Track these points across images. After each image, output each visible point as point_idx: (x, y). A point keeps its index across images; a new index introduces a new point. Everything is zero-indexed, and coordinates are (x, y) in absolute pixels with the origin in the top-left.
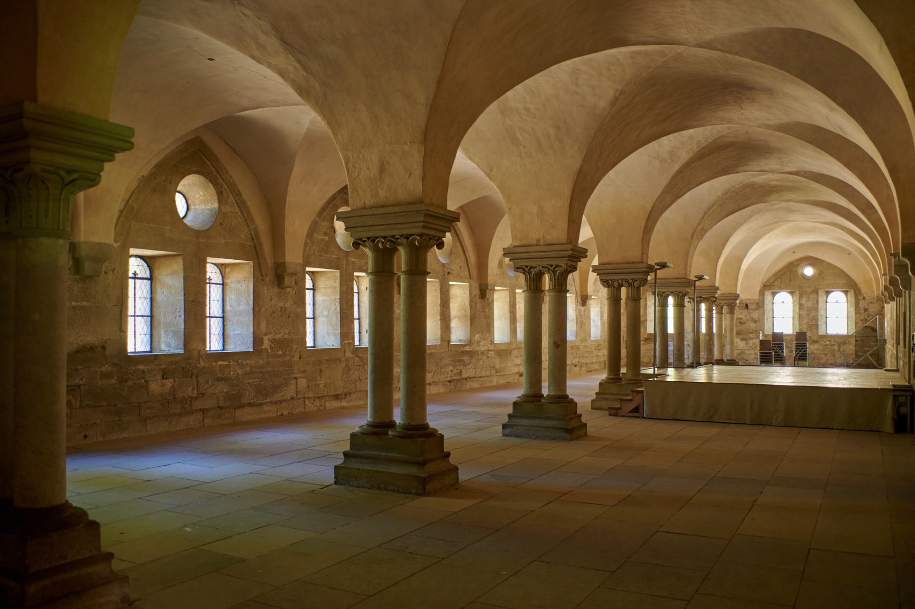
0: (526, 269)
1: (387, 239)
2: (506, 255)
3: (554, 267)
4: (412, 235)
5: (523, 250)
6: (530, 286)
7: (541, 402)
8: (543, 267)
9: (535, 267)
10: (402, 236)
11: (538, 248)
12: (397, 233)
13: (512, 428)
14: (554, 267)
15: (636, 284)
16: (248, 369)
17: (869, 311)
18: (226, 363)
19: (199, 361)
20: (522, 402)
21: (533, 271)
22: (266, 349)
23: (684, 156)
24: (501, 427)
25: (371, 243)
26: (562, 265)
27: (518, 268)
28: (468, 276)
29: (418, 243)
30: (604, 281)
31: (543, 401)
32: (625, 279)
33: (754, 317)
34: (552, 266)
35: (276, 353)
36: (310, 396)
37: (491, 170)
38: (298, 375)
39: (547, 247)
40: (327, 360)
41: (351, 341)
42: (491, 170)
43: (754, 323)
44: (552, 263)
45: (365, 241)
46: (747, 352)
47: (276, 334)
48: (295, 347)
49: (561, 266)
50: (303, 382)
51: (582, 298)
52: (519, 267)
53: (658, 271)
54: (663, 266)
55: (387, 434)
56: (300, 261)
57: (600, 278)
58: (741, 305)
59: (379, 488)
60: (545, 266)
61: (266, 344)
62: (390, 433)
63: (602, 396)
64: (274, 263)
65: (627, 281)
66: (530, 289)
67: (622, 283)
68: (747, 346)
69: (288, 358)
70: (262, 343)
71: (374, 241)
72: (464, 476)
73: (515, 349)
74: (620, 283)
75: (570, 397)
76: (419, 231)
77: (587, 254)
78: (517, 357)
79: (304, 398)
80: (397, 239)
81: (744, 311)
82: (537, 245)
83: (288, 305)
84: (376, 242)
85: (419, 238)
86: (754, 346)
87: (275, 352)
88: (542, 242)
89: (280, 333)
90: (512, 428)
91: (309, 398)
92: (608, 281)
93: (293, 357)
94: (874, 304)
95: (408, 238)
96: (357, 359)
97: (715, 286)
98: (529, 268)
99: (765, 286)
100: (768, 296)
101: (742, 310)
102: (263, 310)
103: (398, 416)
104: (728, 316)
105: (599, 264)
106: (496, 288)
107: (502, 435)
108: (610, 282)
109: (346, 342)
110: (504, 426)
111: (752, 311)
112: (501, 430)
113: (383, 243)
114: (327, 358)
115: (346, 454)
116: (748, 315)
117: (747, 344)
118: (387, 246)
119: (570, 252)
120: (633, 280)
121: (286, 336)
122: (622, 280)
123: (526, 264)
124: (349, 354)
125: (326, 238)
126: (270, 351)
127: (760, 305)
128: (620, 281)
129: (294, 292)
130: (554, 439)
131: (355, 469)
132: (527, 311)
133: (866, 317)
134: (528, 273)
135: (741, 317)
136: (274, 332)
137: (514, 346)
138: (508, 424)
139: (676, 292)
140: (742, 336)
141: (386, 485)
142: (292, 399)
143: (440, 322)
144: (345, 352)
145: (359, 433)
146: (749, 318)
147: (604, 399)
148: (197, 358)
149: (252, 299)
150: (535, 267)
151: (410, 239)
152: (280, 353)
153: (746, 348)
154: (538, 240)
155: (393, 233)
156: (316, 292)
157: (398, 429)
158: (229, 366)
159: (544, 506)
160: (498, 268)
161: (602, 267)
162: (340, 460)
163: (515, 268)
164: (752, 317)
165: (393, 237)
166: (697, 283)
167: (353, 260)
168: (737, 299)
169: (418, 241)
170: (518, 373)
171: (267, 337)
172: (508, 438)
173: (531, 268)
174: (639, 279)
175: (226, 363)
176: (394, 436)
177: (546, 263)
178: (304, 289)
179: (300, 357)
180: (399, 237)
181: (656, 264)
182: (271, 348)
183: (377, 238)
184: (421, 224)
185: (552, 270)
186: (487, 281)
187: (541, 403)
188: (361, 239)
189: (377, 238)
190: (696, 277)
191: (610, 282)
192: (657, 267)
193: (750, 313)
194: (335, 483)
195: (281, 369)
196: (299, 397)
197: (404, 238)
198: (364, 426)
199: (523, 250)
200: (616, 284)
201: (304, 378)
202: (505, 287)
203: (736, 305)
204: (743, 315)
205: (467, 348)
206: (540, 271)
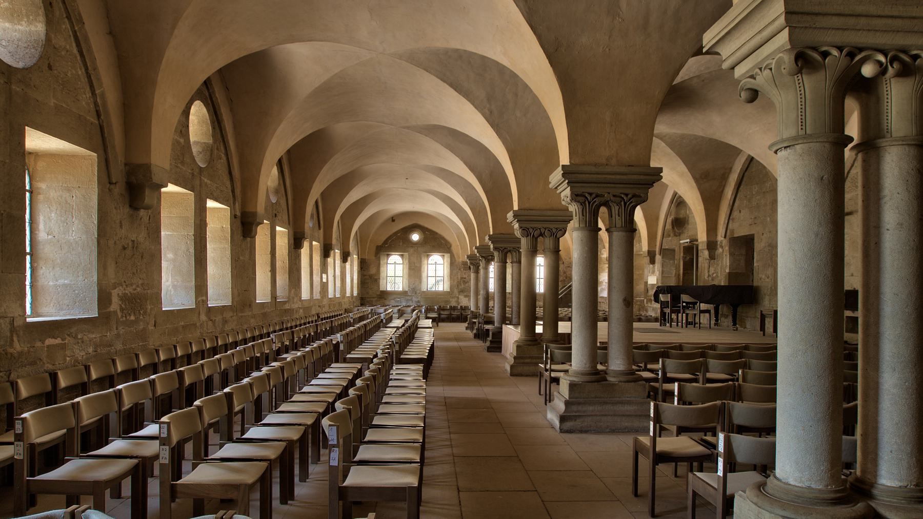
2: (566, 175)
3: (629, 196)
5: (593, 169)
6: (590, 221)
7: (607, 380)
8: (614, 196)
11: (609, 169)
14: (629, 196)
16: (91, 350)
17: (567, 273)
18: (58, 341)
19: (12, 340)
20: (582, 382)
22: (115, 312)
26: (641, 195)
27: (577, 195)
28: (287, 223)
30: (523, 230)
31: (611, 379)
32: (548, 228)
34: (627, 195)
35: (128, 318)
40: (183, 327)
41: (204, 298)
42: (557, 50)
45: (825, 55)
47: (127, 286)
48: (149, 307)
49: (641, 197)
58: (466, 266)
61: (115, 305)
63: (522, 361)
64: (126, 164)
69: (141, 327)
70: (110, 303)
71: (851, 55)
74: (543, 233)
83: (141, 238)
84: (857, 58)
87: (126, 317)
89: (132, 285)
90: (575, 420)
93: (148, 324)
96: (210, 323)
98: (594, 196)
101: (466, 270)
102: (111, 243)
105: (519, 209)
108: (531, 230)
114: (183, 324)
121: (139, 289)
123: (590, 191)
124: (203, 317)
125: (182, 140)
126: (120, 314)
128: (543, 231)
129: (148, 217)
133: (565, 278)
135: (464, 276)
136: (125, 282)
138: (564, 414)
140: (465, 294)
143: (270, 273)
147: (523, 363)
148: (8, 334)
149: (96, 222)
158: (63, 347)
167: (206, 180)
171: (116, 291)
173: (597, 196)
175: (58, 341)
179: (155, 326)
182: (122, 310)
183: (861, 50)
186: (304, 229)
187: (607, 382)
189: (861, 50)
191: (531, 230)
205: (287, 307)
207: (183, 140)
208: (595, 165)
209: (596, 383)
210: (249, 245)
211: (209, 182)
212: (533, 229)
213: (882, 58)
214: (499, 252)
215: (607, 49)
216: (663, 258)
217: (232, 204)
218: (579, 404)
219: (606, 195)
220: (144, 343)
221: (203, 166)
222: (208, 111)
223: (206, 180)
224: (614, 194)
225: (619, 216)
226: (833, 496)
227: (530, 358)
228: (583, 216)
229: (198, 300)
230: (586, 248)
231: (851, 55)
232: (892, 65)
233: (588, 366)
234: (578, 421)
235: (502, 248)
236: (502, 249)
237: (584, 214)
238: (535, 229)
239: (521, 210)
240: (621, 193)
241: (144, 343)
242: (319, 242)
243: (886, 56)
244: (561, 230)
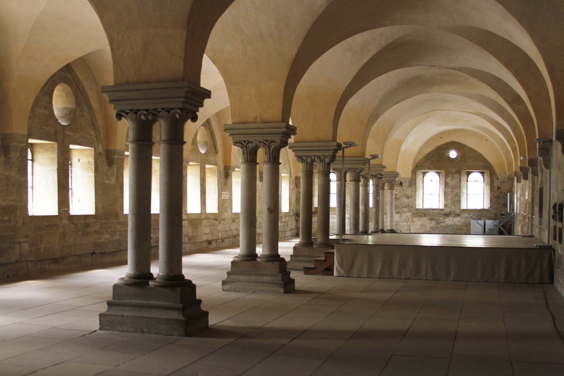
0: (244, 144)
1: (149, 112)
2: (227, 131)
4: (172, 109)
5: (242, 126)
8: (259, 142)
9: (252, 142)
10: (163, 109)
12: (159, 106)
13: (231, 284)
14: (269, 142)
15: (327, 161)
17: (502, 189)
20: (239, 261)
21: (250, 146)
23: (373, 50)
24: (221, 283)
25: (134, 115)
26: (277, 141)
27: (236, 143)
29: (179, 116)
30: (298, 157)
32: (317, 156)
33: (407, 194)
34: (267, 141)
36: (32, 259)
37: (215, 55)
38: (21, 240)
39: (264, 124)
40: (46, 226)
41: (66, 209)
42: (215, 55)
43: (408, 198)
44: (267, 139)
45: (127, 113)
46: (401, 224)
49: (276, 142)
50: (26, 247)
51: (259, 174)
52: (238, 141)
53: (345, 149)
54: (350, 145)
55: (148, 284)
56: (25, 133)
57: (295, 154)
59: (142, 332)
60: (262, 141)
62: (151, 283)
63: (296, 259)
65: (319, 157)
66: (247, 161)
67: (315, 159)
68: (401, 219)
69: (12, 224)
71: (136, 113)
72: (213, 320)
73: (204, 219)
74: (313, 159)
75: (281, 257)
76: (180, 105)
77: (296, 131)
78: (205, 226)
79: (27, 261)
80: (159, 112)
81: (399, 188)
82: (254, 122)
83: (13, 174)
84: (138, 114)
85: (179, 111)
86: (407, 219)
88: (258, 120)
89: (6, 200)
90: (231, 284)
91: (31, 261)
92: (302, 157)
93: (17, 222)
94: (506, 183)
95: (169, 111)
96: (72, 226)
97: (382, 165)
98: (246, 142)
99: (416, 166)
100: (419, 176)
103: (156, 270)
104: (389, 191)
105: (294, 142)
106: (191, 163)
107: (222, 290)
109: (63, 209)
110: (224, 283)
111: (405, 188)
112: (222, 286)
113: (145, 115)
114: (46, 224)
115: (110, 304)
116: (402, 192)
117: (401, 217)
118: (150, 118)
119: (284, 130)
120: (324, 156)
122: (315, 156)
123: (245, 139)
124: (65, 221)
125: (46, 112)
127: (413, 183)
128: (313, 158)
129: (18, 162)
130: (269, 293)
131: (120, 316)
132: (244, 180)
133: (499, 194)
134: (246, 147)
137: (203, 217)
138: (227, 280)
139: (353, 168)
141: (149, 328)
142: (17, 262)
144: (62, 219)
145: (122, 284)
146: (403, 194)
150: (252, 142)
151: (171, 113)
152: (6, 218)
153: (400, 220)
154: (255, 118)
155: (155, 106)
156: (35, 164)
157: (157, 280)
159: (291, 341)
160: (192, 145)
161: (298, 144)
162: (104, 308)
163: (235, 143)
164: (405, 193)
165: (155, 110)
166: (371, 161)
167: (68, 133)
168: (396, 177)
169: (179, 113)
170: (207, 241)
172: (227, 292)
173: (248, 143)
174: (329, 156)
176: (155, 286)
177: (261, 138)
178: (27, 160)
179: (23, 224)
180: (161, 110)
181: (345, 143)
183: (140, 110)
184: (183, 99)
185: (267, 144)
187: (256, 262)
188: (124, 111)
189: (140, 110)
190: (371, 156)
191: (304, 158)
192: (344, 146)
193: (403, 190)
194: (100, 329)
195: (7, 234)
196: (22, 260)
197: (165, 111)
198: (124, 278)
199: (242, 126)
200: (309, 160)
201: (27, 242)
202: (196, 163)
203: (396, 182)
204: (398, 192)
206: (257, 145)
207: (47, 112)
208: (247, 123)
209: (248, 262)
210: (115, 172)
211: (71, 133)
212: (306, 157)
213: (145, 113)
214: (337, 172)
215: (244, 52)
216: (446, 176)
217: (96, 145)
218: (236, 274)
219: (254, 142)
220: (15, 233)
221: (64, 123)
222: (71, 88)
223: (68, 133)
224: (259, 141)
225: (266, 154)
226: (136, 276)
227: (302, 256)
228: (243, 155)
229: (61, 210)
230: (245, 176)
231: (136, 113)
232: (149, 116)
233: (245, 251)
234: (232, 284)
235: (339, 169)
236: (339, 170)
237: (244, 154)
238: (307, 157)
239: (297, 142)
240: (264, 140)
241: (15, 233)
242: (215, 165)
243: (147, 112)
244: (327, 157)
